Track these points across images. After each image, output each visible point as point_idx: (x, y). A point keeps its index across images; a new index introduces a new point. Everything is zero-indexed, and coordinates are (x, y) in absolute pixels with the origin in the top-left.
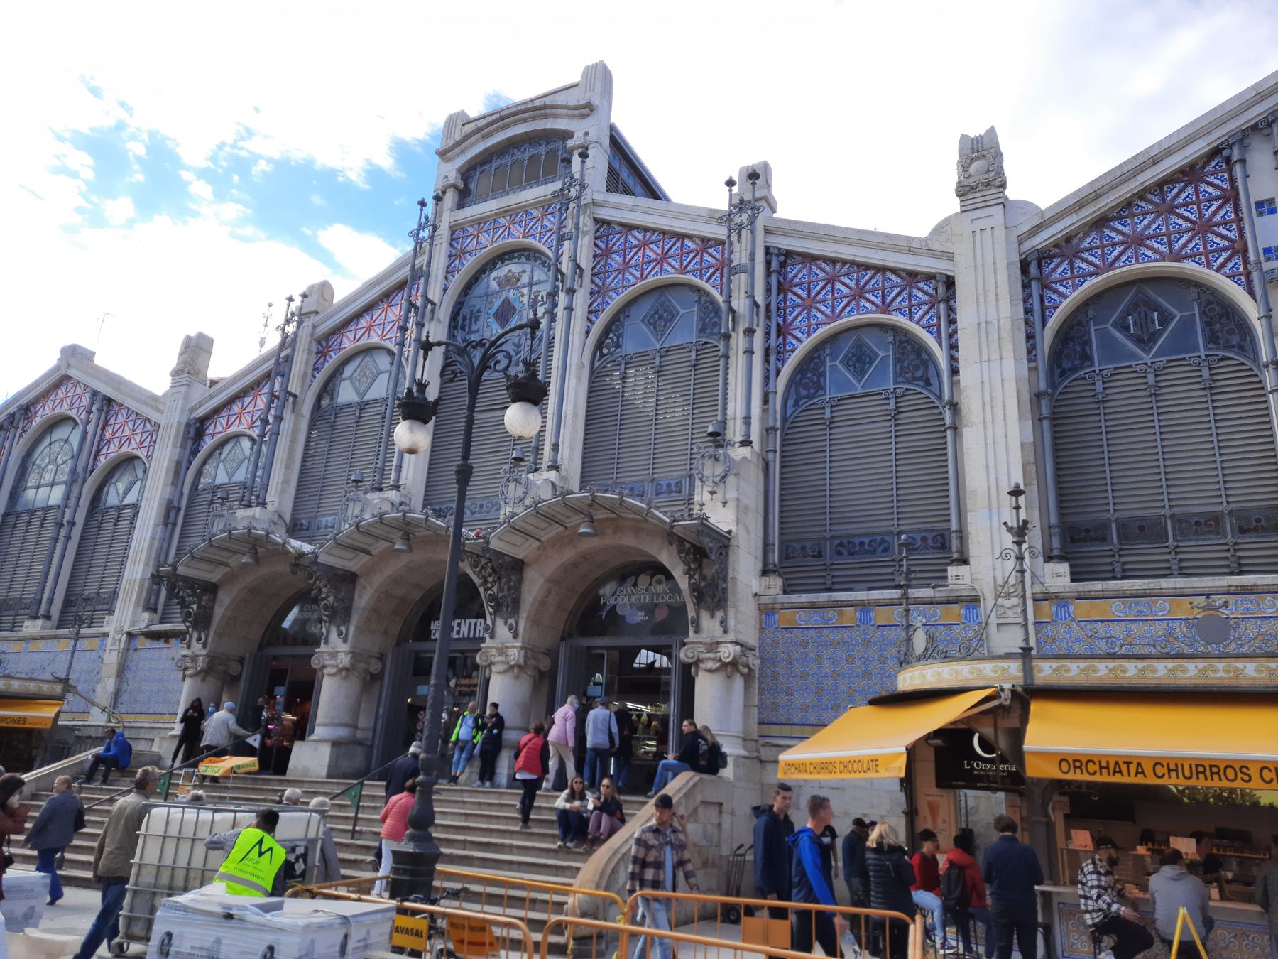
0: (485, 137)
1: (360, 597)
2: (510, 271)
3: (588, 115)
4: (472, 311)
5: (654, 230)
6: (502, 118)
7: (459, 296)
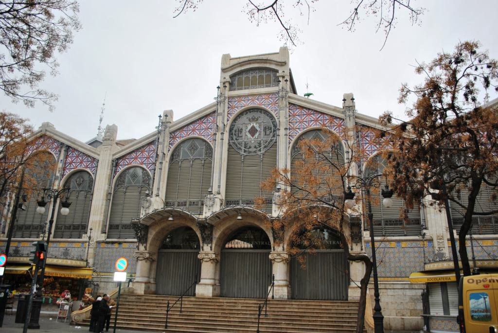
0: (241, 66)
1: (215, 234)
6: (249, 61)
7: (232, 122)
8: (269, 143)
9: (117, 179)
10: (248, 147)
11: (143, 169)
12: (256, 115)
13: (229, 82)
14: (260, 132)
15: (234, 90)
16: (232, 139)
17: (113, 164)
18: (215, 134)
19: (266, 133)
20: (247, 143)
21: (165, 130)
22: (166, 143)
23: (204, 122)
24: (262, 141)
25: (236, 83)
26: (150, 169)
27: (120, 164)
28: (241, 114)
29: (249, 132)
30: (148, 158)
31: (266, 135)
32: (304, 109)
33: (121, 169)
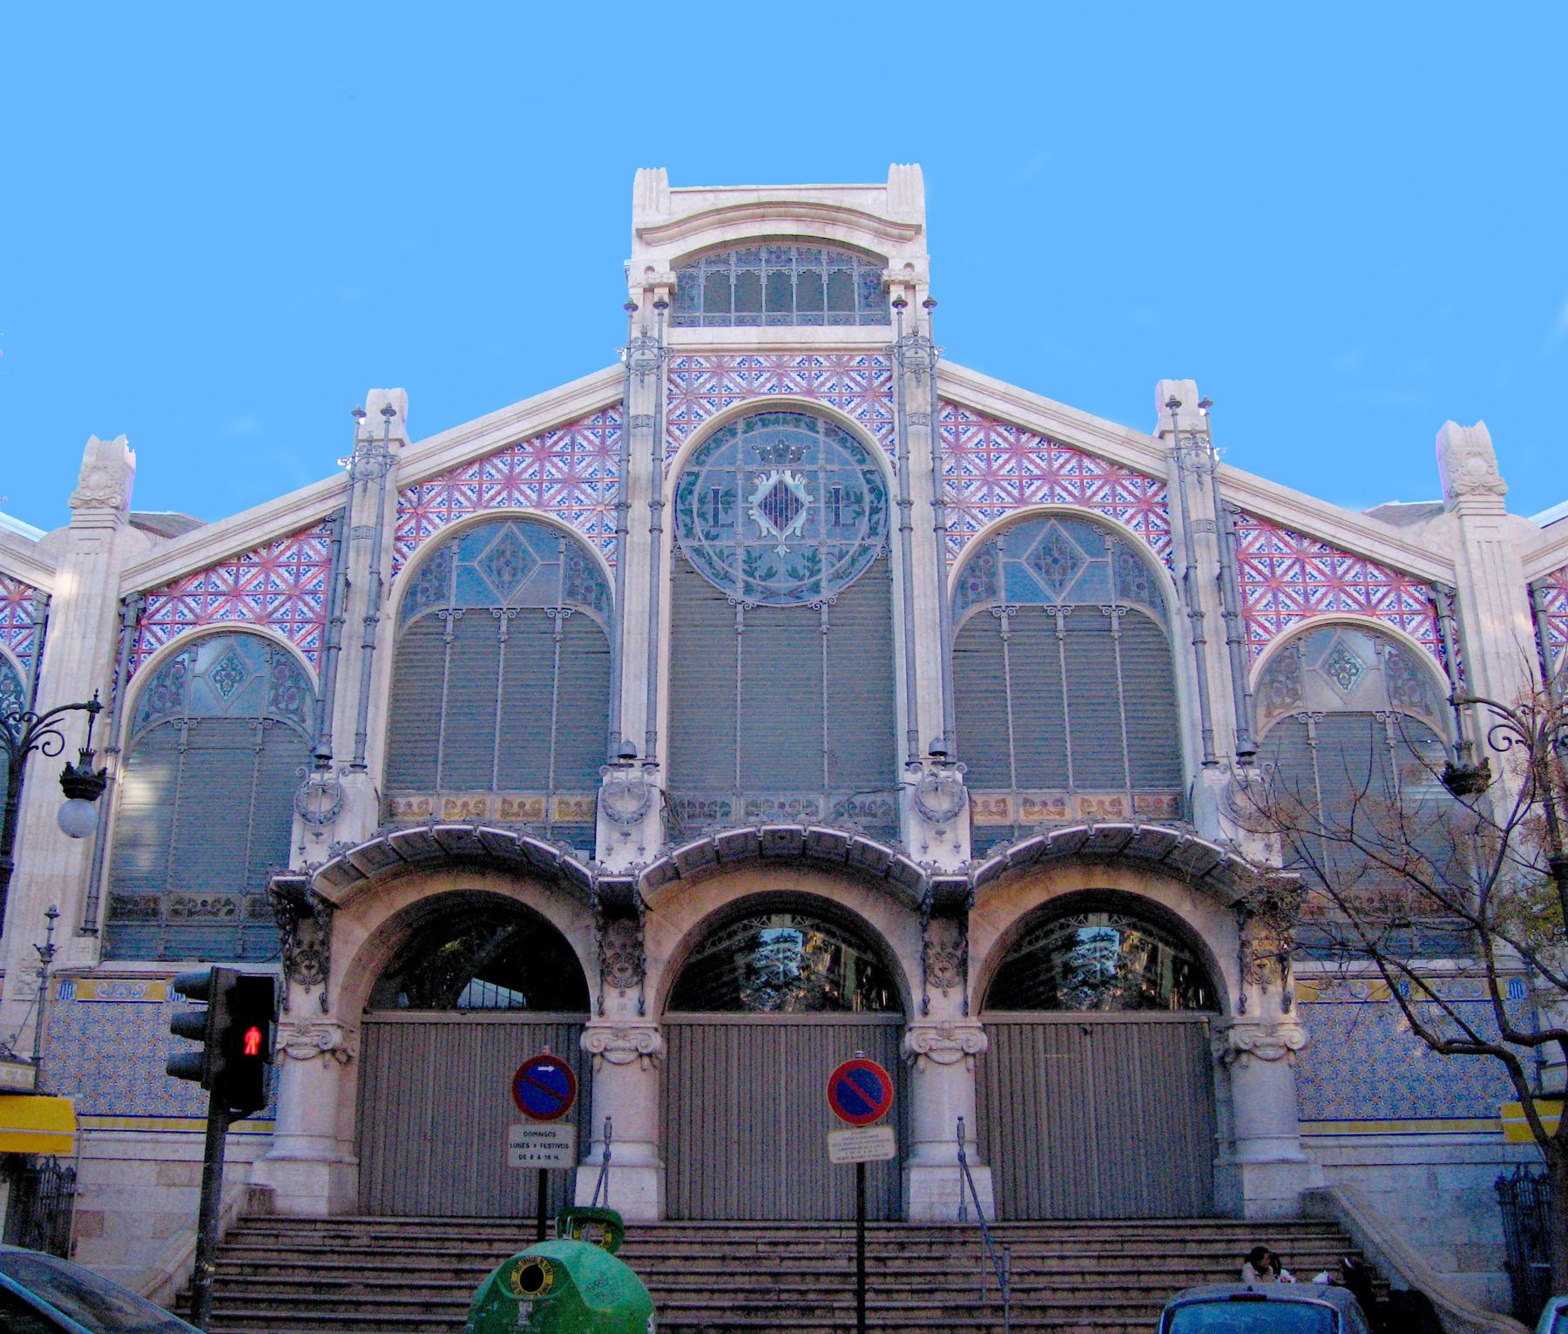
0: (723, 224)
1: (658, 943)
3: (910, 240)
5: (1034, 434)
7: (687, 461)
8: (854, 560)
9: (145, 687)
13: (671, 287)
14: (814, 512)
15: (693, 323)
16: (689, 533)
17: (122, 617)
18: (622, 506)
19: (837, 515)
20: (755, 554)
23: (557, 449)
24: (824, 550)
25: (699, 293)
26: (304, 643)
27: (158, 617)
28: (724, 431)
29: (766, 506)
30: (297, 593)
31: (837, 523)
32: (1001, 429)
33: (160, 644)
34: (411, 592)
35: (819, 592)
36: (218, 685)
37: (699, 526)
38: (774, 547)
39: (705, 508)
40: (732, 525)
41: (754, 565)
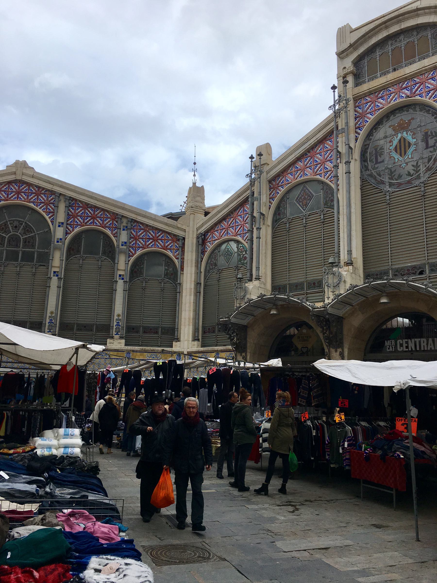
2: (402, 119)
4: (376, 150)
10: (396, 177)
11: (238, 242)
12: (405, 117)
16: (367, 169)
17: (199, 242)
18: (336, 167)
21: (259, 178)
22: (264, 198)
31: (427, 147)
34: (275, 214)
35: (420, 178)
36: (225, 258)
37: (370, 165)
38: (400, 165)
39: (372, 158)
40: (383, 161)
41: (393, 175)
